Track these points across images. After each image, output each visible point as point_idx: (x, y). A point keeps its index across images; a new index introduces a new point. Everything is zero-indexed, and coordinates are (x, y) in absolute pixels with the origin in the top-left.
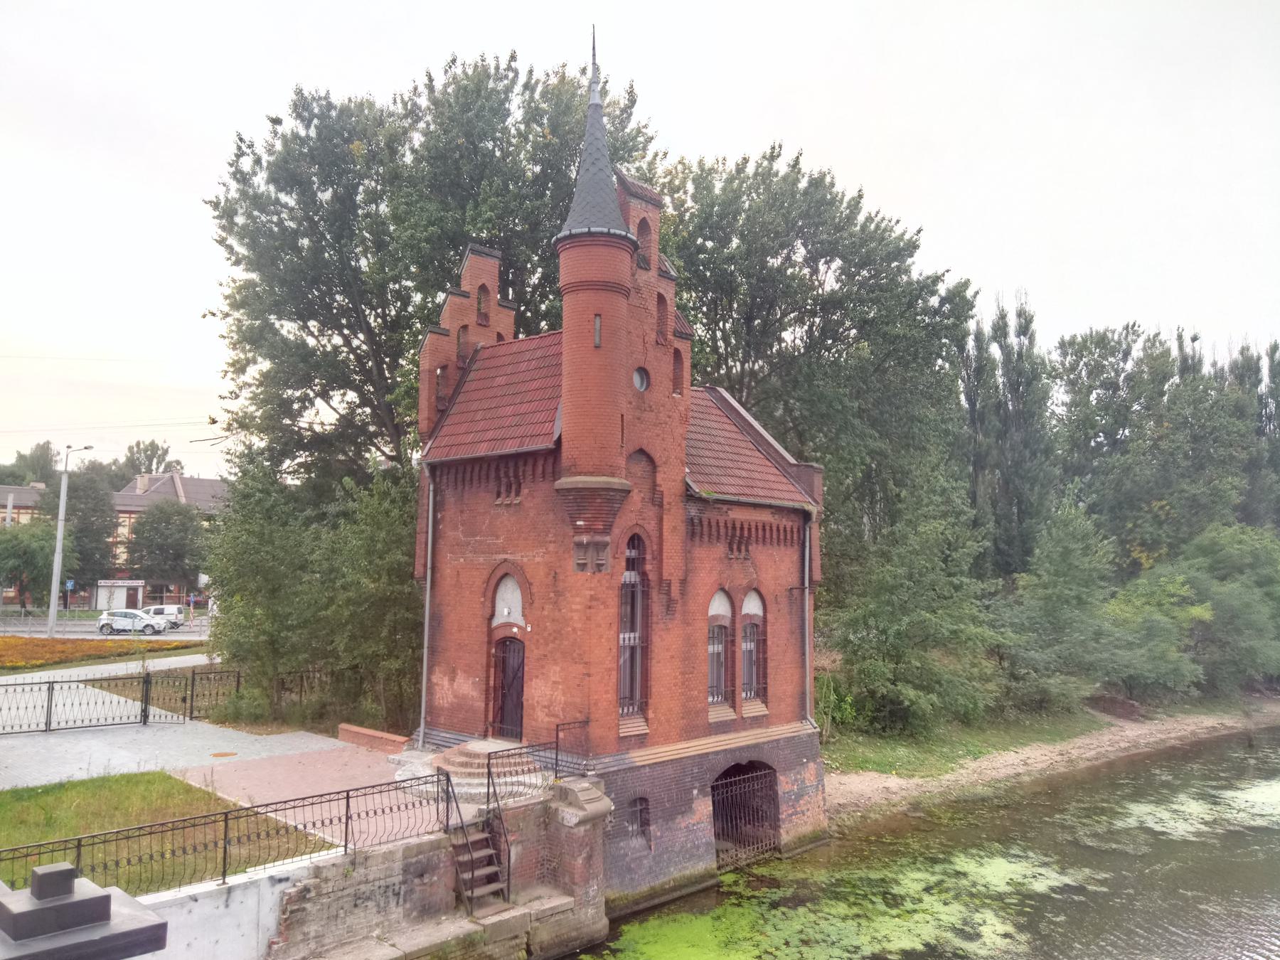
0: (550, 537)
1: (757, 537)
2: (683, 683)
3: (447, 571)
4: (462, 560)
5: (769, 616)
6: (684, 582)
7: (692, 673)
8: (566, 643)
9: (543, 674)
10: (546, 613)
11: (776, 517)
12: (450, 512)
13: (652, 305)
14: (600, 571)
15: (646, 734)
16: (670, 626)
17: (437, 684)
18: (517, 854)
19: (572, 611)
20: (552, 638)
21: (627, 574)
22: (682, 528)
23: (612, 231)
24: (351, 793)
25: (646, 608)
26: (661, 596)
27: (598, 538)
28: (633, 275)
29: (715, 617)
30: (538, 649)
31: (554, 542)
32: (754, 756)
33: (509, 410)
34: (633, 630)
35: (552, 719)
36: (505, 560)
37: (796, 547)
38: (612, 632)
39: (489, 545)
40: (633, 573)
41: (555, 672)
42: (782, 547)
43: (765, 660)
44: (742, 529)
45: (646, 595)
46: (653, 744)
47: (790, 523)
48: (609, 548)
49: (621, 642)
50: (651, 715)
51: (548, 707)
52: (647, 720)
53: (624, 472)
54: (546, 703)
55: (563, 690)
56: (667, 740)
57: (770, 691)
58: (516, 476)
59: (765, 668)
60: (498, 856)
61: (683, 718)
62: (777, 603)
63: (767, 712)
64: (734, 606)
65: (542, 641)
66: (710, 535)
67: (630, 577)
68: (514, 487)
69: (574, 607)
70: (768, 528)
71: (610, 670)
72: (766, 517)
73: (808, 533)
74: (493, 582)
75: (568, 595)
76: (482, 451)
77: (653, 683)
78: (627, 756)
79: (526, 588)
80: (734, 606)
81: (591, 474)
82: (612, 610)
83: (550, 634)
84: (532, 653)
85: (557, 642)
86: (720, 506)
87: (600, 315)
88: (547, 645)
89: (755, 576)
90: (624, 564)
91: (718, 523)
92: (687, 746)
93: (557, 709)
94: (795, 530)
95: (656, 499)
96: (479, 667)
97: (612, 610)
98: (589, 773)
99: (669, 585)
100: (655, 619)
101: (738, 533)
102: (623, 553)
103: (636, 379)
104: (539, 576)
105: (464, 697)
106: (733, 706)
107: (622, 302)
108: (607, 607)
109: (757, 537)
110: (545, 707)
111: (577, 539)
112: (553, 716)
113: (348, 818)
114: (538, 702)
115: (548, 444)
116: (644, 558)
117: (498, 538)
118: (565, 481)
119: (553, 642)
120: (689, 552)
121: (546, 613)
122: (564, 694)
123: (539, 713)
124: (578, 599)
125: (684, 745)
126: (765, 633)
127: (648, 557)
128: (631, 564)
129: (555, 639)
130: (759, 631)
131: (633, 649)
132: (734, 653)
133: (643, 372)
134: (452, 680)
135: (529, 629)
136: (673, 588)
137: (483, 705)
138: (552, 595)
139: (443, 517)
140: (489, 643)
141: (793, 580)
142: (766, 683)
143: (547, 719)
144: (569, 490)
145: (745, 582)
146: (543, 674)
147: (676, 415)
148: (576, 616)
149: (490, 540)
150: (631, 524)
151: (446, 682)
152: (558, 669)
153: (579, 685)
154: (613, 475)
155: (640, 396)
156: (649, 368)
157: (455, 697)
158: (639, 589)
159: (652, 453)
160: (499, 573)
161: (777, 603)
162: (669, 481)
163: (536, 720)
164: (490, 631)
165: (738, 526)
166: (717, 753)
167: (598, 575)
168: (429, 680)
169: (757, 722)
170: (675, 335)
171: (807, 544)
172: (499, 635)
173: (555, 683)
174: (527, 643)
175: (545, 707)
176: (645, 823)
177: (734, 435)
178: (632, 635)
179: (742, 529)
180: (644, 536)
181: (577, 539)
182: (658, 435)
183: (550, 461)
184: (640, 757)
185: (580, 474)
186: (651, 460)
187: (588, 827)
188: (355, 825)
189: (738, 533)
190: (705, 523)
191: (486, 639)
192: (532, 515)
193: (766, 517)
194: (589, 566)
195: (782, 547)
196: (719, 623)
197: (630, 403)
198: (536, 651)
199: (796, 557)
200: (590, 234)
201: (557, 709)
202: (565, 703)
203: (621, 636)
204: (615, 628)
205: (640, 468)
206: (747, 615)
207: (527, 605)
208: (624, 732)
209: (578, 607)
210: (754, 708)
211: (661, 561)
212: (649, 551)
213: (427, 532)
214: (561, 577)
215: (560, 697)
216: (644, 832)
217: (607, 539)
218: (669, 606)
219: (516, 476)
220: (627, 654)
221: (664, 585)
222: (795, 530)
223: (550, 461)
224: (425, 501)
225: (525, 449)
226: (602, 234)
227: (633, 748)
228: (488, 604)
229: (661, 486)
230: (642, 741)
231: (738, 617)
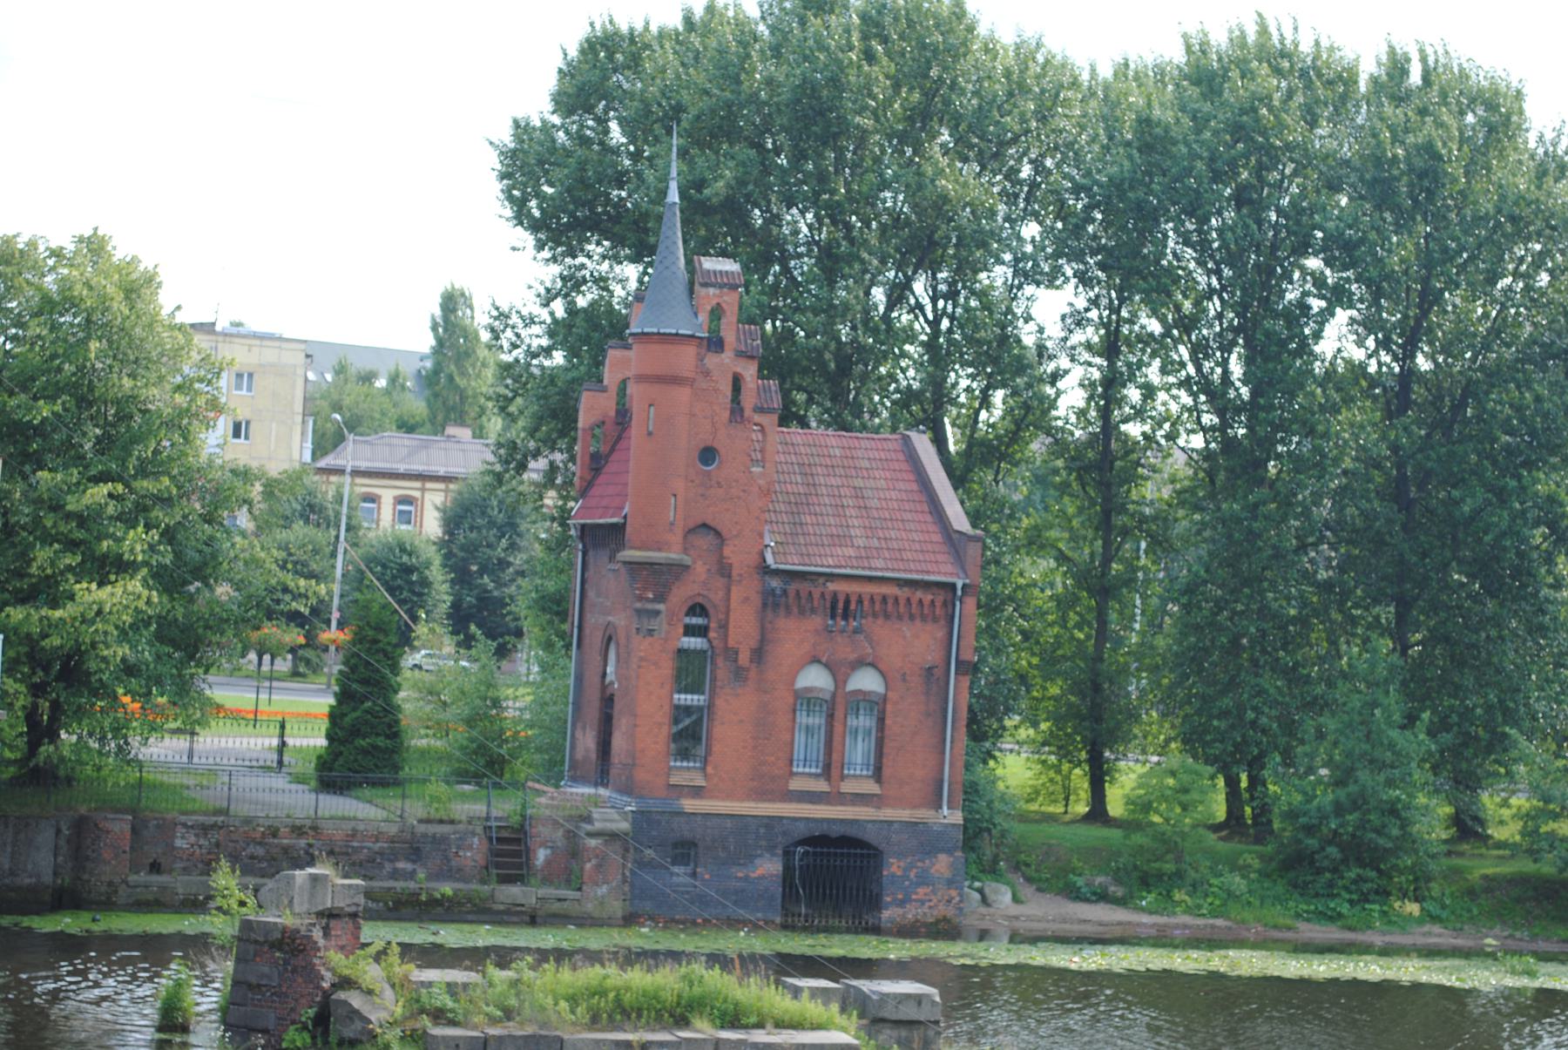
6: (759, 654)
13: (727, 389)
21: (686, 639)
22: (757, 600)
27: (650, 606)
32: (852, 832)
37: (943, 622)
42: (918, 622)
46: (711, 797)
48: (663, 616)
50: (709, 770)
56: (729, 796)
57: (886, 772)
62: (904, 680)
64: (840, 680)
81: (639, 548)
90: (681, 630)
95: (724, 570)
107: (683, 394)
125: (753, 804)
127: (713, 625)
130: (877, 706)
136: (741, 656)
145: (853, 657)
154: (660, 550)
159: (719, 528)
161: (904, 680)
162: (738, 555)
167: (650, 639)
180: (708, 606)
184: (689, 805)
186: (718, 534)
199: (940, 634)
200: (643, 334)
206: (859, 692)
208: (675, 779)
221: (732, 654)
226: (653, 334)
230: (697, 792)
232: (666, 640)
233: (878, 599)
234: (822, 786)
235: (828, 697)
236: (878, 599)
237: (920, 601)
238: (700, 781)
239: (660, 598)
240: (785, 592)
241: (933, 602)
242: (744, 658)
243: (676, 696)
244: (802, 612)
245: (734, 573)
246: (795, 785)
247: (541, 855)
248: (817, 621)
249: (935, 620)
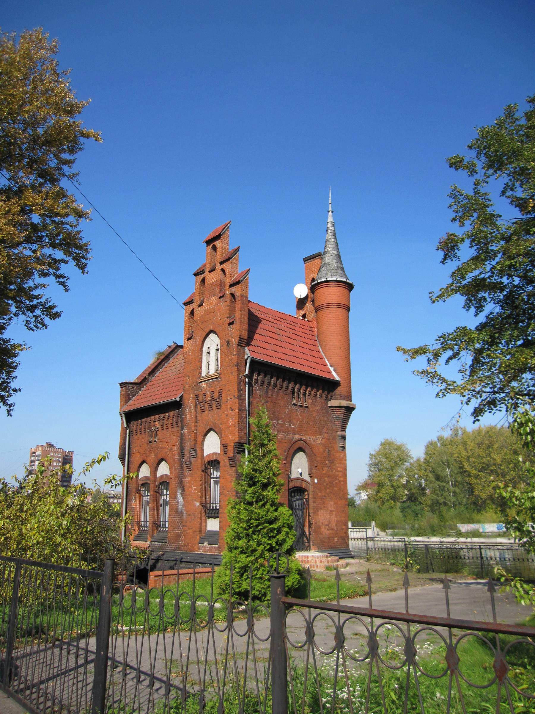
0: (325, 430)
8: (336, 489)
10: (324, 472)
19: (338, 471)
20: (328, 486)
30: (321, 492)
31: (327, 433)
35: (331, 532)
36: (301, 440)
39: (288, 428)
41: (331, 505)
51: (328, 525)
54: (327, 523)
69: (339, 469)
93: (333, 525)
110: (326, 525)
114: (322, 523)
121: (324, 472)
122: (336, 517)
138: (327, 462)
143: (328, 532)
149: (288, 425)
152: (332, 503)
153: (343, 511)
163: (322, 534)
173: (331, 511)
175: (326, 525)
198: (319, 494)
201: (333, 525)
202: (338, 521)
215: (334, 519)
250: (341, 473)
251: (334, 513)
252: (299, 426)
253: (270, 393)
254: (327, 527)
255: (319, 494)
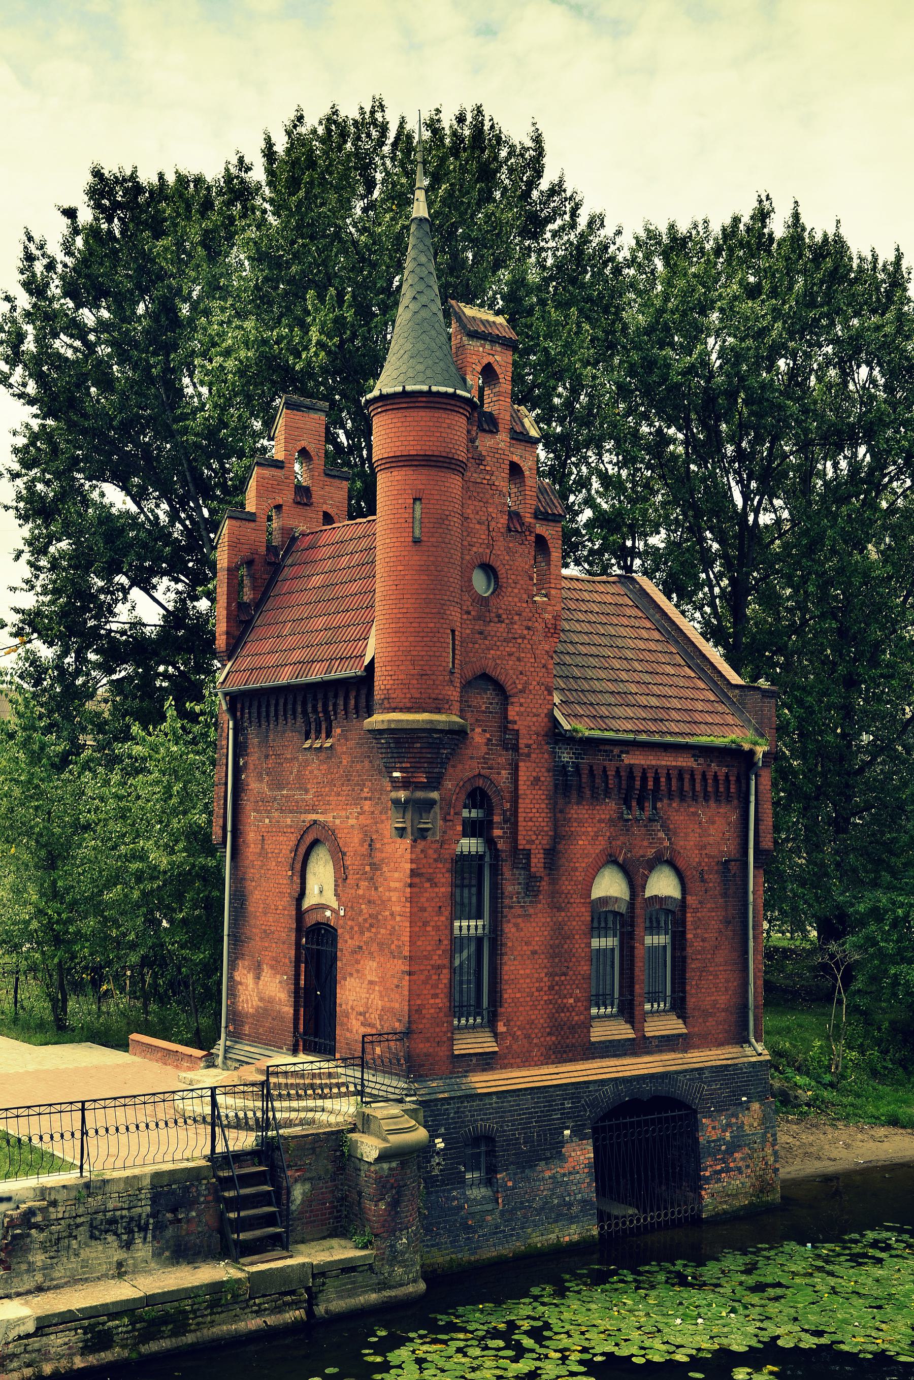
0: (366, 793)
1: (670, 789)
2: (551, 988)
3: (251, 836)
4: (267, 821)
5: (689, 898)
6: (552, 854)
7: (565, 974)
8: (383, 931)
9: (358, 971)
10: (360, 892)
11: (701, 761)
12: (253, 758)
14: (424, 838)
15: (495, 1053)
16: (531, 911)
17: (240, 983)
18: (304, 1194)
20: (367, 925)
21: (465, 841)
22: (546, 778)
23: (434, 389)
24: (87, 1104)
25: (496, 888)
26: (516, 872)
27: (420, 794)
28: (472, 441)
29: (604, 900)
30: (352, 938)
31: (370, 799)
33: (320, 622)
34: (479, 916)
36: (315, 822)
37: (735, 802)
38: (443, 919)
39: (297, 802)
40: (473, 841)
41: (371, 968)
42: (712, 804)
43: (684, 959)
44: (644, 779)
45: (496, 871)
46: (504, 1067)
47: (725, 770)
48: (437, 808)
49: (456, 932)
50: (501, 1028)
52: (496, 1035)
53: (456, 706)
54: (361, 1009)
55: (380, 992)
56: (526, 1062)
57: (691, 1002)
58: (326, 711)
59: (684, 971)
60: (278, 1192)
61: (549, 1034)
62: (703, 880)
63: (685, 1031)
64: (635, 885)
65: (356, 929)
66: (593, 788)
67: (470, 845)
68: (324, 726)
70: (687, 777)
71: (439, 967)
72: (685, 761)
73: (753, 783)
74: (302, 850)
75: (385, 869)
76: (285, 677)
77: (505, 987)
78: (464, 1080)
79: (338, 856)
80: (635, 885)
81: (409, 710)
82: (443, 890)
83: (365, 920)
84: (346, 944)
85: (374, 930)
86: (607, 748)
87: (420, 499)
88: (362, 933)
89: (667, 843)
90: (459, 828)
91: (605, 770)
92: (556, 1071)
93: (374, 1017)
94: (732, 779)
96: (287, 961)
97: (443, 890)
98: (408, 1099)
99: (528, 854)
100: (507, 901)
101: (638, 784)
102: (458, 814)
103: (479, 582)
104: (353, 843)
105: (271, 1000)
106: (631, 1021)
107: (455, 482)
108: (434, 885)
109: (670, 789)
110: (361, 1014)
111: (394, 795)
112: (369, 1025)
113: (84, 1133)
114: (352, 1008)
115: (358, 671)
116: (491, 822)
117: (307, 791)
118: (379, 719)
119: (369, 930)
120: (561, 811)
121: (360, 892)
123: (354, 1022)
124: (396, 875)
125: (552, 1069)
126: (683, 922)
127: (497, 819)
128: (472, 829)
129: (371, 926)
131: (479, 940)
132: (632, 949)
133: (489, 570)
134: (258, 977)
135: (342, 913)
136: (534, 861)
137: (289, 1010)
138: (368, 868)
139: (245, 763)
140: (299, 930)
141: (729, 848)
142: (684, 991)
144: (381, 732)
145: (650, 853)
146: (358, 971)
147: (540, 626)
148: (394, 896)
150: (468, 774)
151: (249, 980)
153: (397, 986)
154: (438, 711)
155: (484, 602)
156: (496, 564)
157: (261, 999)
158: (487, 859)
159: (502, 678)
160: (309, 839)
161: (703, 880)
164: (300, 915)
165: (638, 774)
166: (602, 1082)
167: (421, 845)
168: (231, 978)
169: (668, 1043)
170: (536, 517)
171: (753, 798)
172: (310, 920)
173: (371, 983)
174: (340, 931)
175: (361, 1014)
176: (492, 1170)
177: (652, 646)
178: (480, 923)
179: (644, 779)
181: (394, 795)
182: (510, 655)
183: (363, 692)
185: (394, 710)
186: (500, 689)
187: (394, 1165)
188: (92, 1142)
189: (638, 784)
190: (585, 772)
191: (294, 926)
192: (345, 762)
193: (685, 761)
194: (409, 830)
195: (712, 804)
196: (610, 908)
197: (468, 613)
198: (350, 941)
200: (404, 393)
201: (374, 1017)
203: (457, 924)
204: (446, 912)
205: (484, 700)
207: (340, 881)
208: (460, 1048)
209: (397, 885)
210: (672, 1025)
211: (516, 823)
212: (497, 811)
213: (226, 784)
214: (378, 846)
216: (489, 1182)
217: (435, 795)
218: (531, 887)
219: (326, 711)
220: (473, 948)
221: (521, 857)
222: (732, 779)
223: (363, 692)
224: (224, 743)
225: (333, 675)
226: (420, 393)
227: (473, 1071)
228: (297, 880)
229: (515, 722)
230: (487, 1061)
231: (639, 900)
232: (442, 843)
233: (673, 774)
234: (622, 1031)
235: (623, 909)
236: (673, 774)
237: (716, 776)
238: (489, 1045)
239: (434, 783)
240: (577, 766)
241: (727, 776)
242: (537, 862)
243: (457, 924)
244: (595, 797)
245: (522, 742)
246: (598, 1033)
247: (298, 1193)
248: (610, 808)
249: (728, 800)
250: (397, 894)
251: (377, 988)
252: (318, 795)
253: (271, 737)
254: (361, 1018)
255: (350, 941)
